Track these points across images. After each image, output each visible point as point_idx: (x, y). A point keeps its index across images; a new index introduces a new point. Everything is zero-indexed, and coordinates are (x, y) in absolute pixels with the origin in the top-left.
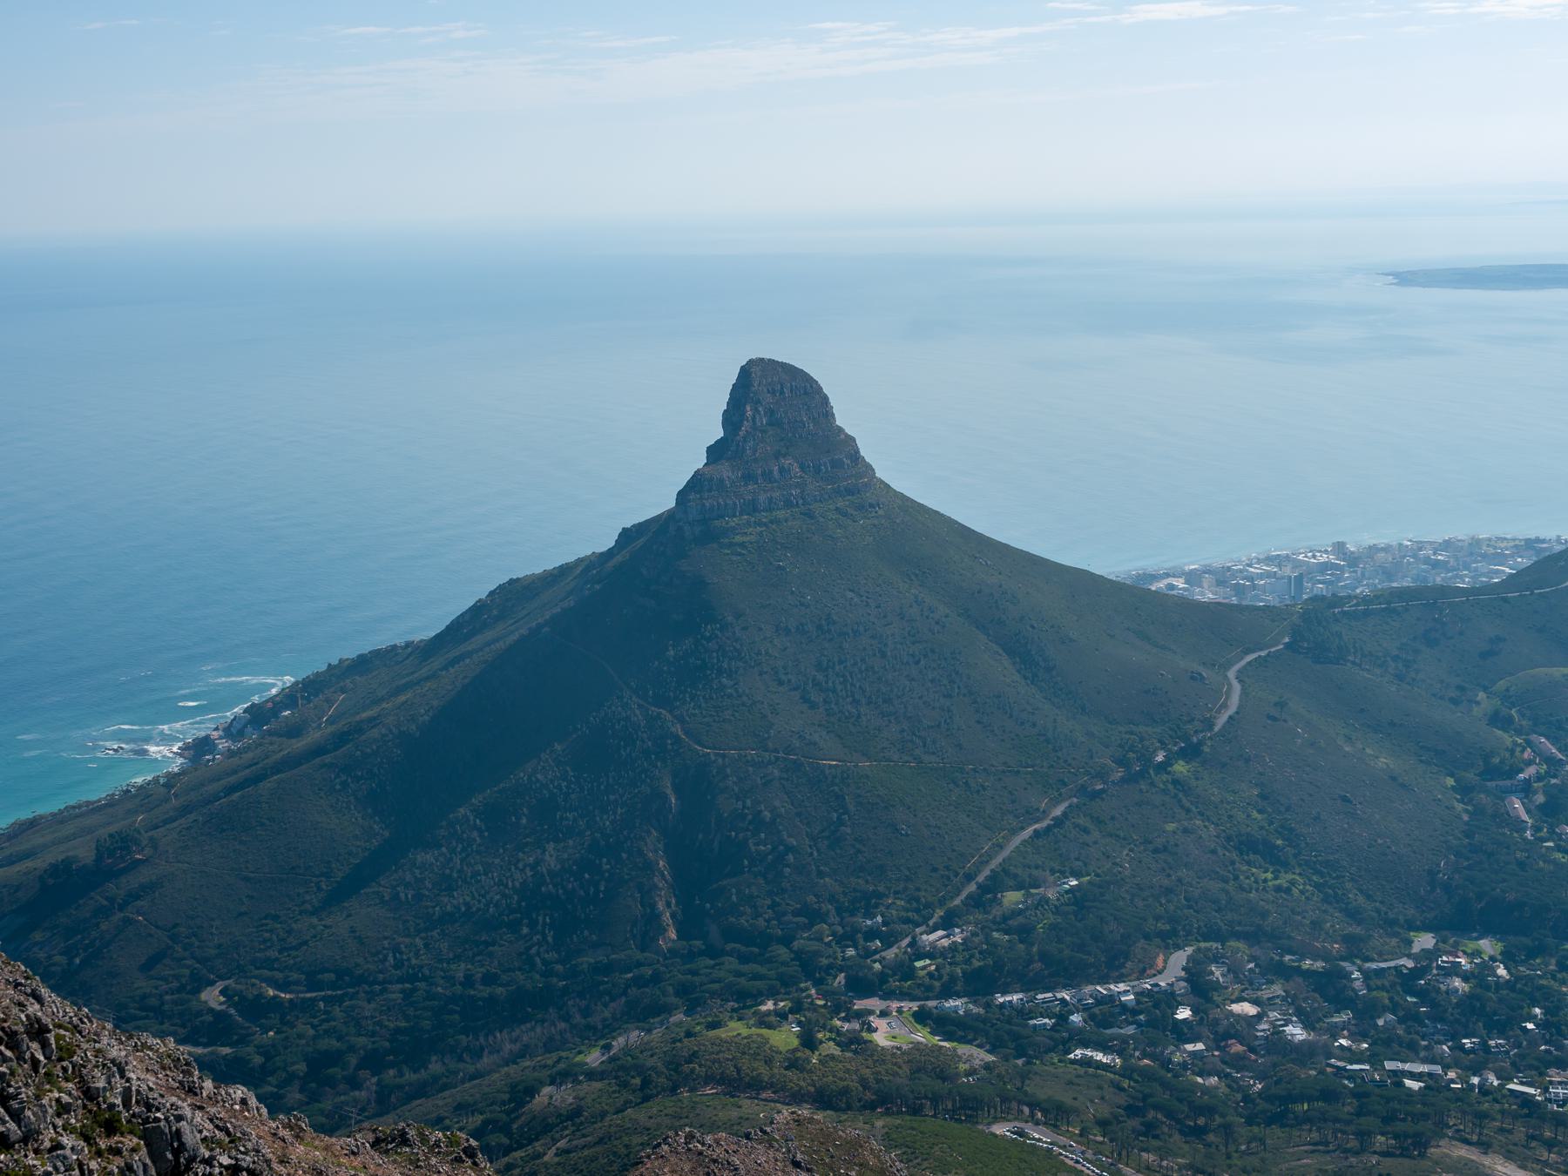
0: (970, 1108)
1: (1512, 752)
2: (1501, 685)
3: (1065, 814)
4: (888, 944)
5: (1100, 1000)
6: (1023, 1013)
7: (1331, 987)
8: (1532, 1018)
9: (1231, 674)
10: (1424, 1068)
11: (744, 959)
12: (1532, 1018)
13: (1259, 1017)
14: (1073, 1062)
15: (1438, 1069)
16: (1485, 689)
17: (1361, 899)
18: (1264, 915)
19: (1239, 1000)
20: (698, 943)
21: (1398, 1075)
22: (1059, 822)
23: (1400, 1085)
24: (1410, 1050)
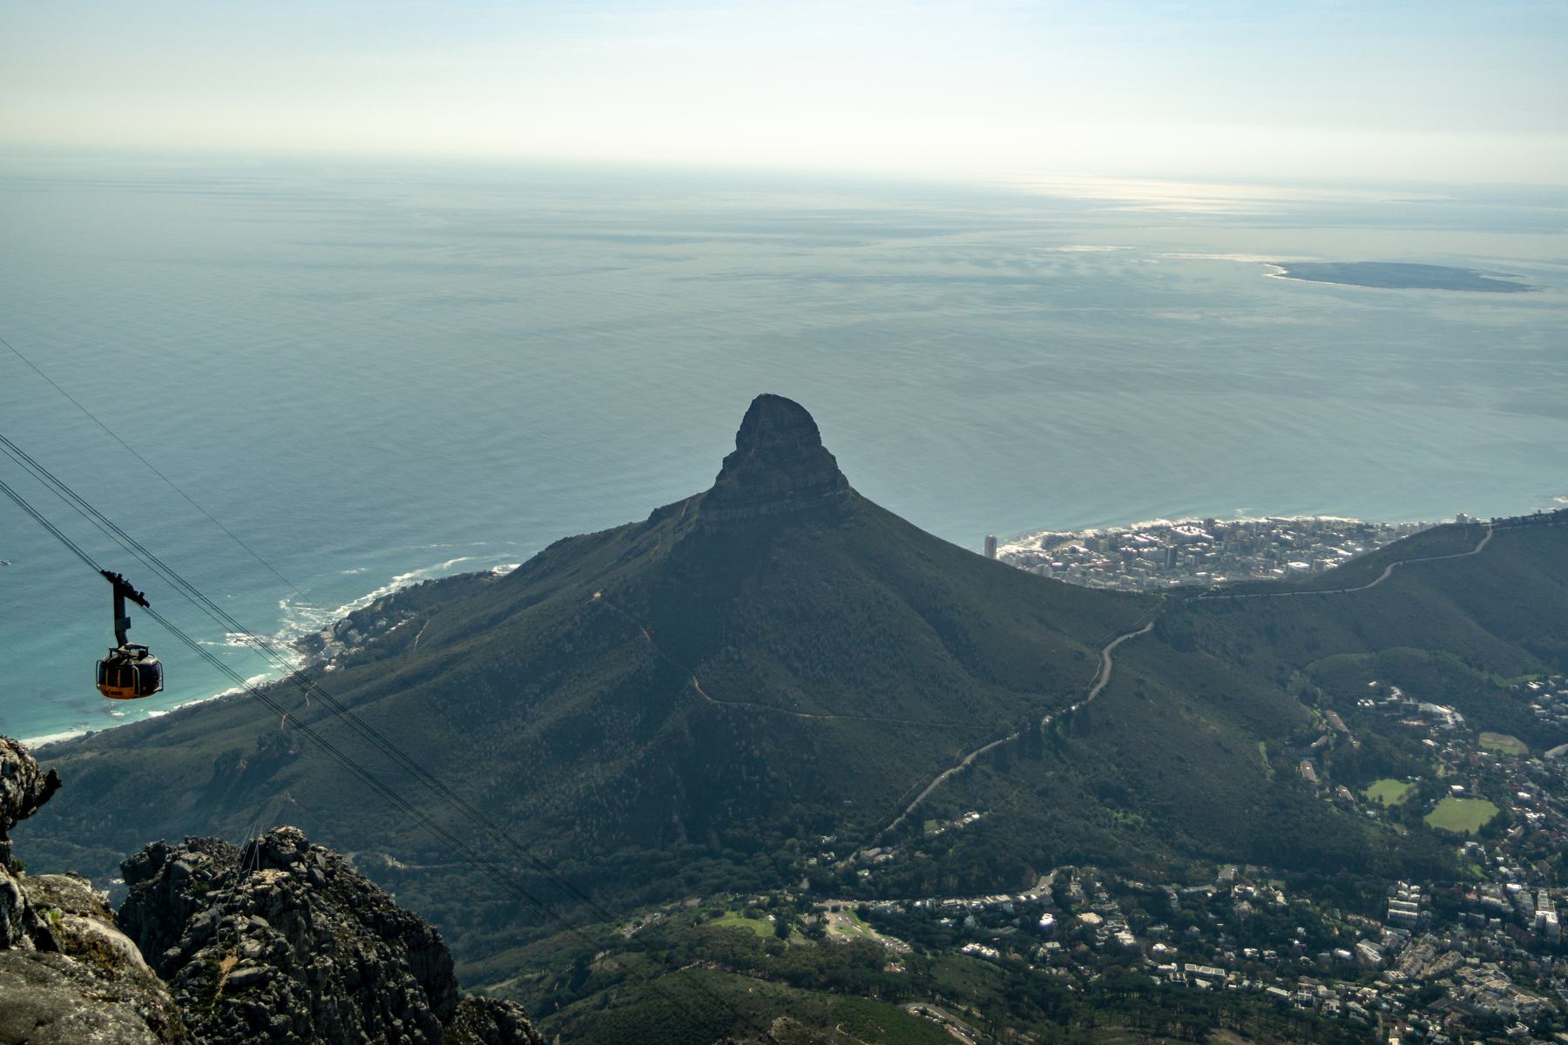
0: (894, 992)
1: (1311, 725)
2: (1311, 667)
3: (973, 762)
4: (841, 858)
5: (989, 908)
6: (935, 914)
7: (1156, 906)
8: (1297, 936)
9: (1106, 652)
10: (1212, 971)
11: (738, 862)
12: (1297, 936)
13: (1101, 925)
14: (966, 953)
15: (1222, 972)
16: (1299, 668)
17: (1185, 838)
18: (1113, 847)
19: (1088, 911)
20: (702, 846)
21: (1193, 975)
22: (970, 769)
23: (1193, 984)
24: (1208, 957)
